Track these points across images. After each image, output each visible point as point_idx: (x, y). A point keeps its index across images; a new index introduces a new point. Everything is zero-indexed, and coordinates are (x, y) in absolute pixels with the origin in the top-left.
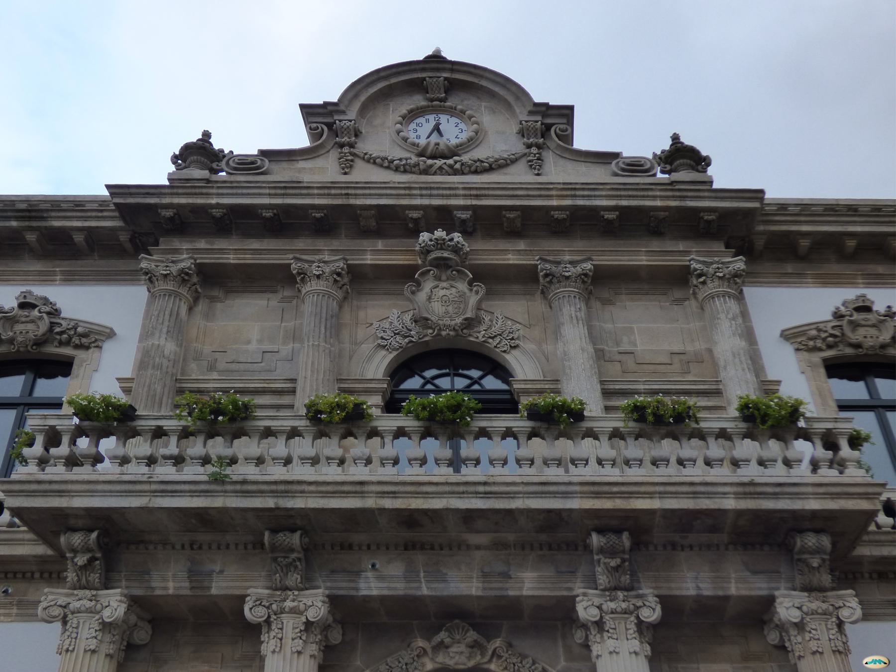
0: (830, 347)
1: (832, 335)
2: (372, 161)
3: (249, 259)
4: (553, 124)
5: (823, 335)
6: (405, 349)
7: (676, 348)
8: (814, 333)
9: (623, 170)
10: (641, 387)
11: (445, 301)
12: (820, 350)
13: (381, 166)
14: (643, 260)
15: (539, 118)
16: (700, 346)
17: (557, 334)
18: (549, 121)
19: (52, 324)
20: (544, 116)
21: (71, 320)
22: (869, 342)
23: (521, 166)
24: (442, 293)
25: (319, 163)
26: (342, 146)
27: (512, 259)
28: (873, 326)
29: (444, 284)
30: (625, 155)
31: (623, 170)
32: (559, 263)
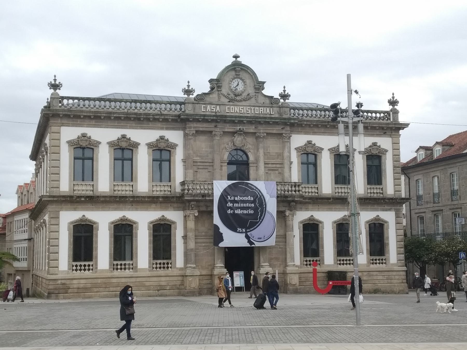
0: (303, 151)
1: (303, 149)
3: (204, 129)
7: (277, 151)
13: (227, 98)
14: (275, 132)
16: (281, 151)
17: (258, 150)
24: (239, 139)
26: (219, 91)
27: (252, 131)
29: (239, 137)
30: (275, 97)
32: (260, 133)
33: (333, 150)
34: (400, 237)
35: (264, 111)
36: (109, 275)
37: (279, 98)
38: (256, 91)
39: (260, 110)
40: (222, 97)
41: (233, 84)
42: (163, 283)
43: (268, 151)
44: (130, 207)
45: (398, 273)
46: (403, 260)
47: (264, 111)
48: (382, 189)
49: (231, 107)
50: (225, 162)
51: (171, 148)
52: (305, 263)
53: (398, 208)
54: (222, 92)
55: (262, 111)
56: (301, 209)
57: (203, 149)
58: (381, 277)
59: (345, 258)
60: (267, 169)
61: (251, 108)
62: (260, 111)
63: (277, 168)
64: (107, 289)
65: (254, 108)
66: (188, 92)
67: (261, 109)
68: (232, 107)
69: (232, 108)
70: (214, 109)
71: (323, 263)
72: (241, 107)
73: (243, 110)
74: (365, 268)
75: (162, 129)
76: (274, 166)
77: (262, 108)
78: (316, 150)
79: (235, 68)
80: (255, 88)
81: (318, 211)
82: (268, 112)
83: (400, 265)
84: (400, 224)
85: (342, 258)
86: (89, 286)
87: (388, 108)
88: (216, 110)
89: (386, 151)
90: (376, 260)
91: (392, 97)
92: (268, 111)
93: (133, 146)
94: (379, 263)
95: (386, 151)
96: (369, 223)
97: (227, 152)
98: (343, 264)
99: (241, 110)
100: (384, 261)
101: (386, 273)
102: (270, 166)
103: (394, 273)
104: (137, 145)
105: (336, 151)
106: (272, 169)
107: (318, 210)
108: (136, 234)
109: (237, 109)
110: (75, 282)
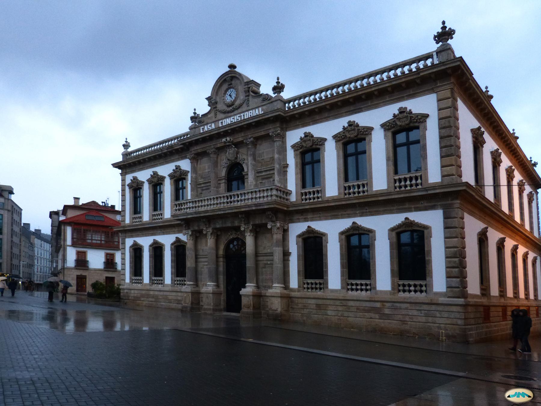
5: (299, 146)
6: (228, 166)
8: (297, 145)
9: (263, 101)
10: (263, 170)
12: (299, 150)
15: (247, 86)
18: (249, 86)
19: (181, 171)
22: (308, 146)
23: (245, 105)
24: (230, 152)
28: (309, 140)
29: (230, 149)
31: (263, 101)
33: (339, 137)
34: (452, 249)
36: (148, 287)
39: (249, 113)
40: (218, 113)
42: (179, 298)
43: (263, 158)
44: (160, 232)
45: (447, 308)
46: (458, 287)
48: (421, 176)
50: (222, 179)
52: (306, 286)
53: (449, 202)
54: (217, 109)
55: (251, 114)
56: (299, 221)
57: (206, 170)
58: (415, 313)
59: (359, 282)
60: (261, 178)
63: (271, 175)
64: (148, 299)
65: (243, 114)
67: (251, 113)
71: (327, 287)
74: (388, 297)
76: (268, 173)
77: (250, 112)
78: (316, 143)
81: (320, 220)
83: (450, 294)
84: (451, 229)
85: (354, 282)
86: (139, 295)
87: (434, 47)
90: (410, 286)
94: (415, 291)
96: (396, 231)
97: (224, 169)
98: (357, 290)
100: (424, 288)
101: (425, 307)
102: (264, 174)
103: (440, 308)
106: (266, 177)
107: (320, 219)
108: (164, 254)
110: (132, 292)
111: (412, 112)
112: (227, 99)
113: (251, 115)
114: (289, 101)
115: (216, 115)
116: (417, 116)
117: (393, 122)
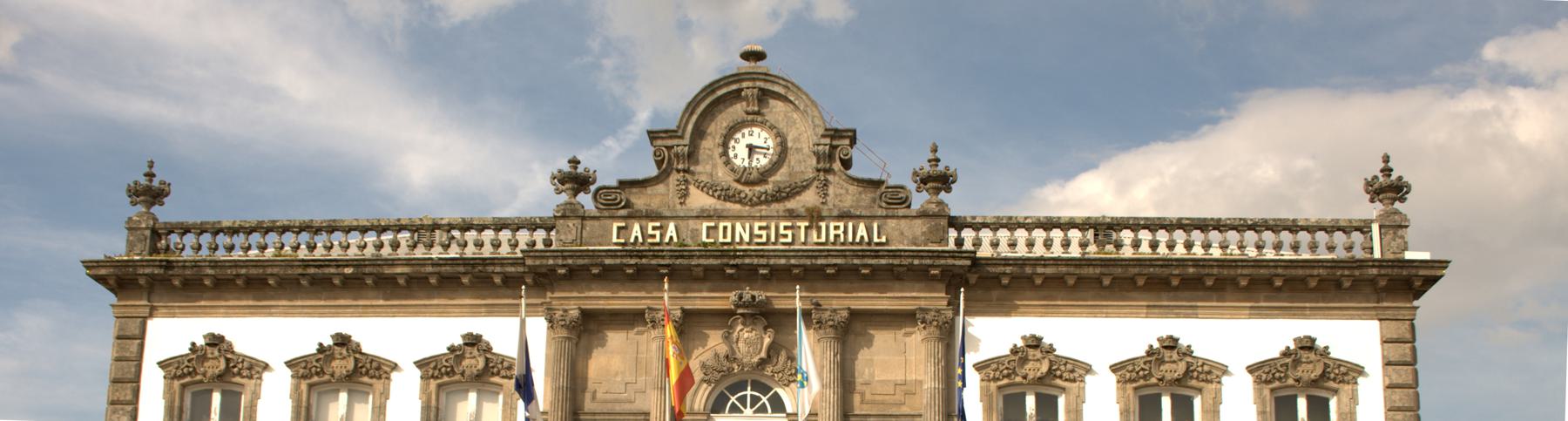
2: (703, 187)
4: (838, 146)
5: (1001, 368)
11: (748, 342)
15: (828, 141)
18: (835, 143)
20: (832, 138)
21: (499, 355)
24: (746, 335)
25: (660, 188)
29: (748, 329)
35: (845, 232)
37: (912, 186)
38: (819, 166)
41: (734, 147)
47: (845, 232)
49: (721, 225)
51: (503, 377)
55: (840, 232)
61: (799, 224)
62: (832, 232)
66: (576, 181)
67: (836, 228)
68: (725, 224)
69: (725, 228)
70: (658, 233)
72: (757, 225)
73: (764, 233)
75: (474, 311)
77: (837, 224)
79: (742, 90)
80: (816, 154)
82: (862, 237)
88: (662, 236)
89: (1359, 371)
91: (1382, 171)
92: (862, 231)
93: (371, 372)
95: (1359, 371)
99: (757, 232)
104: (388, 369)
105: (1141, 373)
109: (742, 231)
111: (1329, 353)
112: (736, 156)
113: (837, 236)
114: (957, 224)
115: (685, 195)
116: (1340, 366)
117: (1281, 366)
